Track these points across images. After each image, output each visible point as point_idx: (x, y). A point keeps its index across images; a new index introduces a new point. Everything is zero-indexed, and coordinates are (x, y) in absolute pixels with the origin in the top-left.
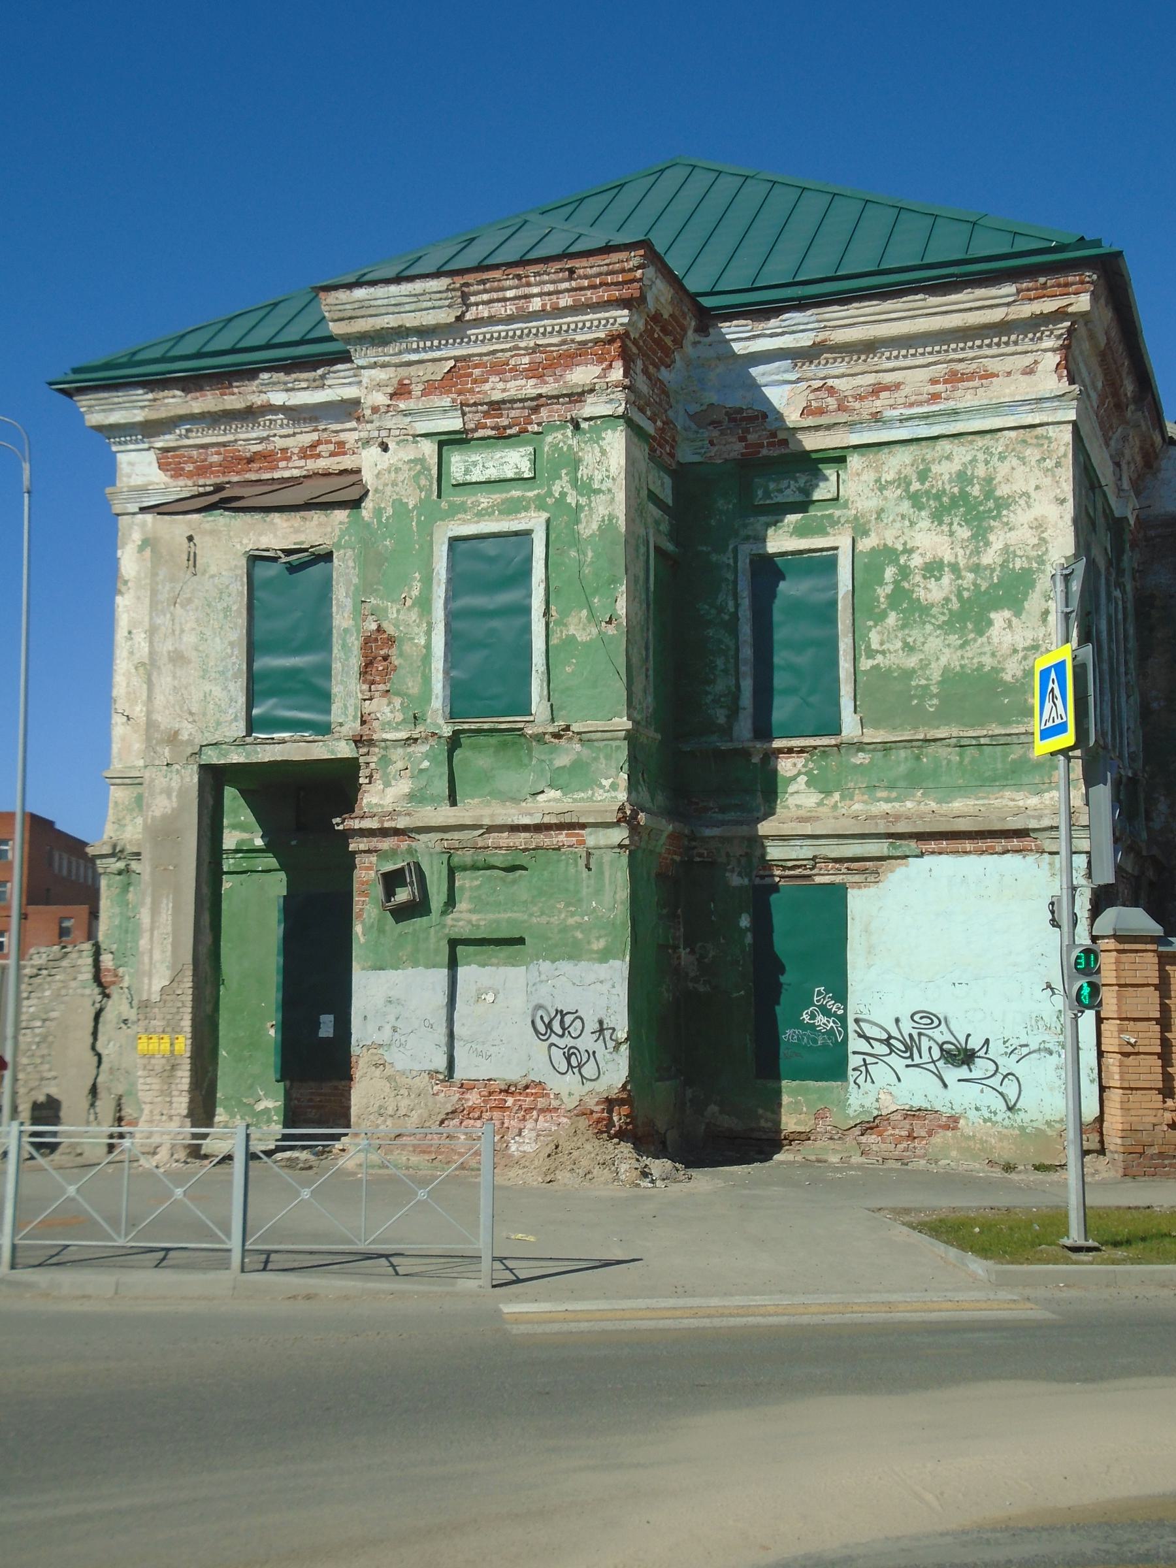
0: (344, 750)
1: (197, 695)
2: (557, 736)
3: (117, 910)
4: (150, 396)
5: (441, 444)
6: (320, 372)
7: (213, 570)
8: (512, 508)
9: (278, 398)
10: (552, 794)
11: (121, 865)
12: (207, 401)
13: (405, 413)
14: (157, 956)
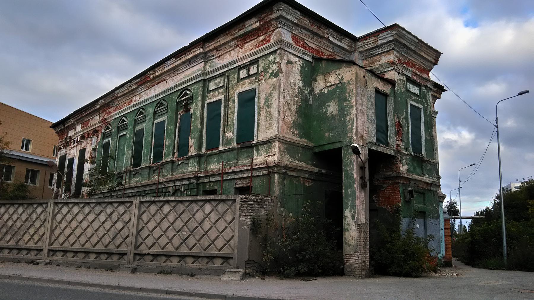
0: (392, 153)
1: (367, 126)
2: (427, 161)
3: (281, 187)
4: (301, 17)
5: (407, 79)
6: (343, 37)
7: (369, 89)
8: (417, 102)
9: (331, 38)
10: (427, 176)
11: (284, 171)
12: (314, 28)
13: (404, 67)
14: (361, 208)
